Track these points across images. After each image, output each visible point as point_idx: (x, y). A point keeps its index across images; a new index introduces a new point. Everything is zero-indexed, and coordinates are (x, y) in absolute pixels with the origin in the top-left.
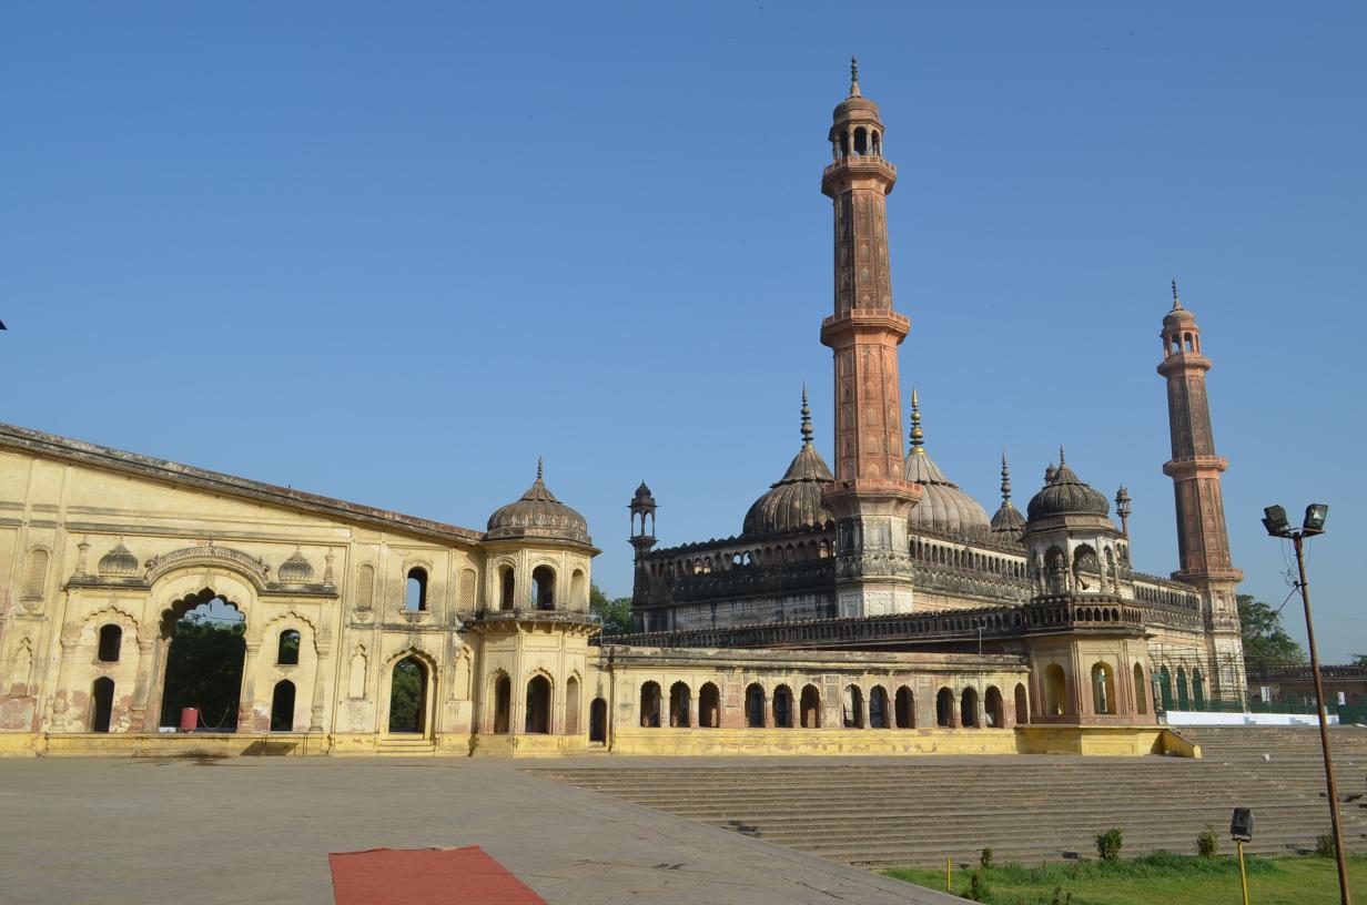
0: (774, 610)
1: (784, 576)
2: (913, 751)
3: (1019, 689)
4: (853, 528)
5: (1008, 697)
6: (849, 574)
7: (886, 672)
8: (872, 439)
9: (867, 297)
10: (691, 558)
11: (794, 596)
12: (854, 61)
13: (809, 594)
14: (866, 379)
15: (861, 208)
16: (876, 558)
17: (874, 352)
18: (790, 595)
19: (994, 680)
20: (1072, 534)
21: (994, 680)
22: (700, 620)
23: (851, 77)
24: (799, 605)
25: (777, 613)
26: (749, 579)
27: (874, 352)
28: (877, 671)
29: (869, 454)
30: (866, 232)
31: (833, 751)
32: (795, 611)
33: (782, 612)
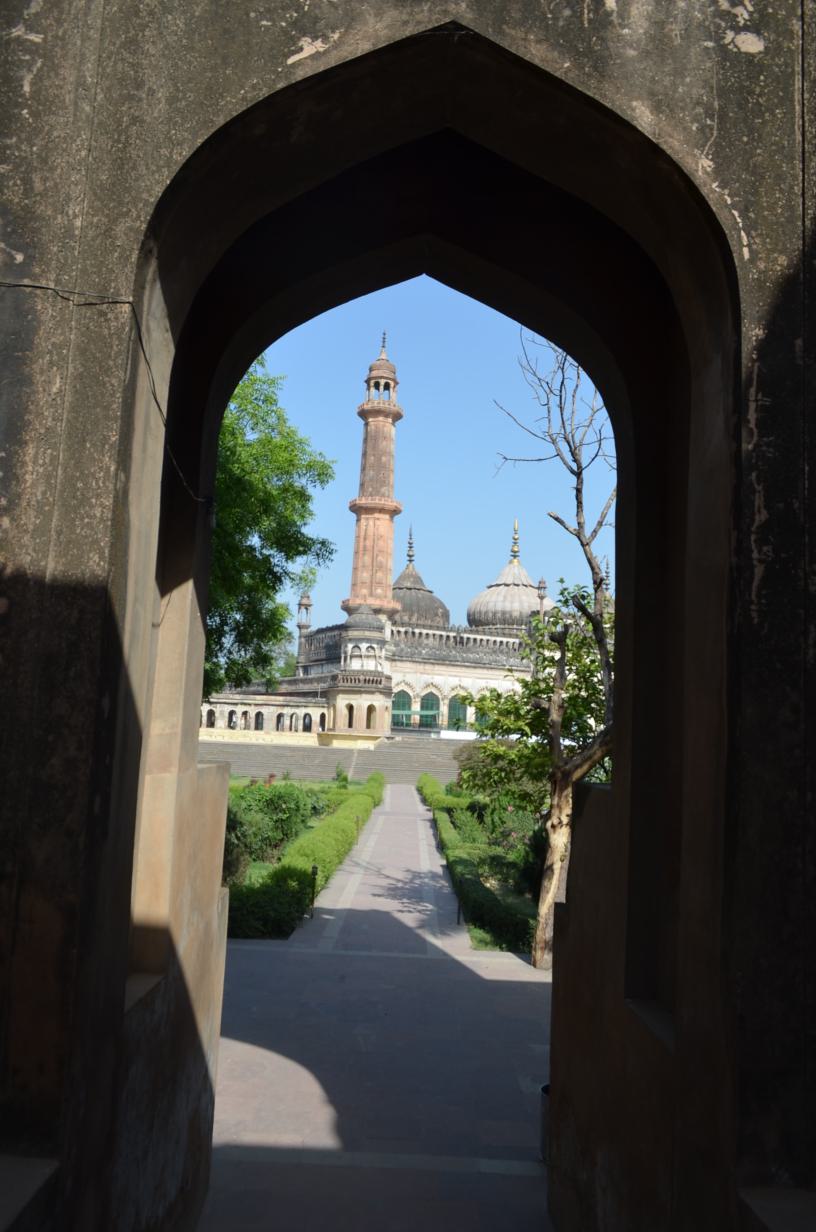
2: (261, 742)
3: (323, 716)
5: (316, 719)
7: (250, 705)
8: (365, 575)
9: (370, 489)
14: (365, 539)
15: (373, 434)
17: (371, 523)
19: (309, 710)
20: (350, 640)
21: (309, 710)
27: (371, 523)
28: (245, 704)
30: (374, 448)
31: (220, 739)
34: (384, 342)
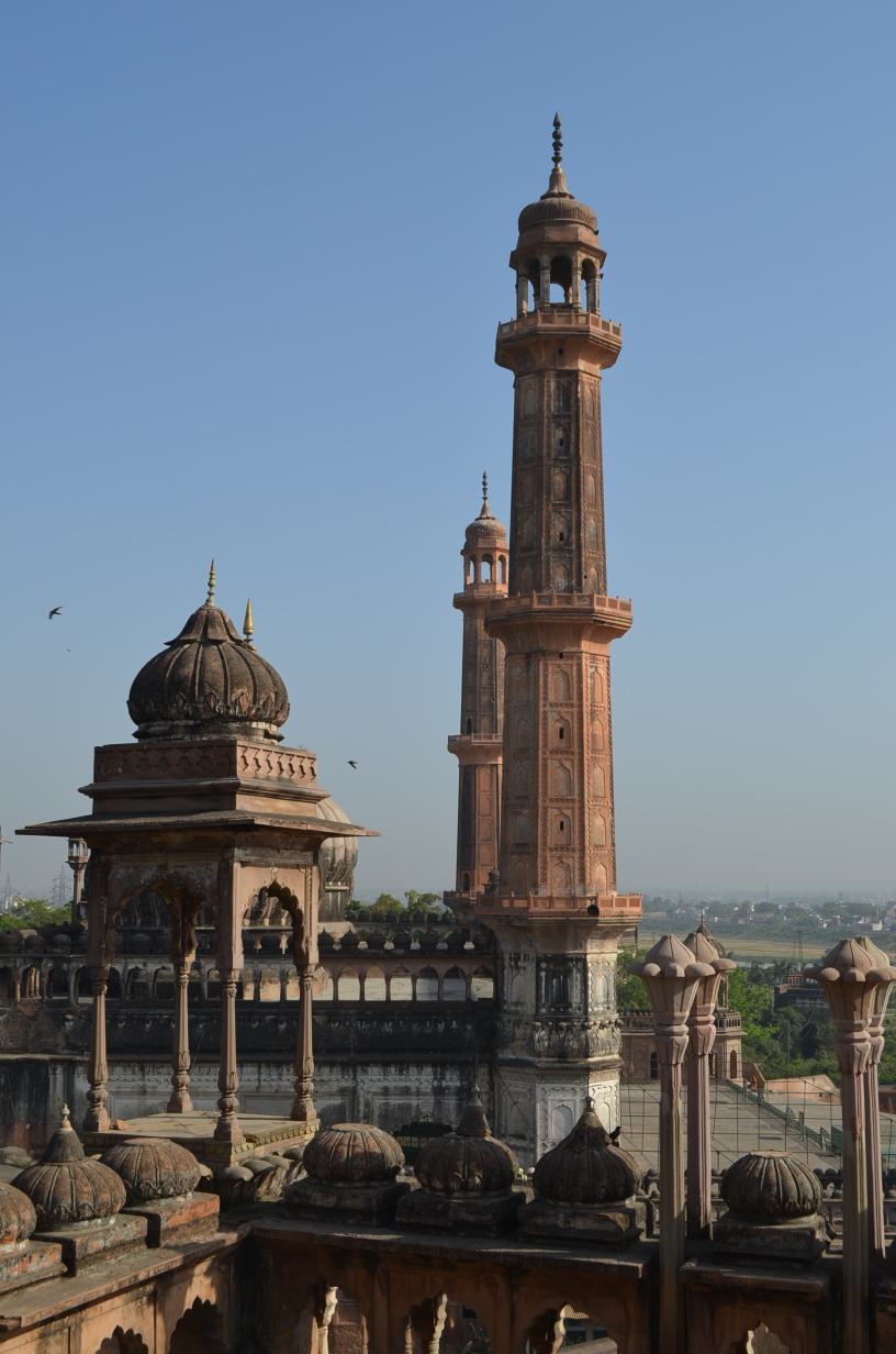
0: (335, 1087)
1: (365, 1026)
4: (568, 973)
6: (562, 1053)
10: (119, 968)
11: (385, 1065)
12: (557, 124)
13: (420, 1065)
16: (602, 1026)
18: (376, 1063)
22: (143, 1092)
23: (552, 153)
24: (394, 1080)
25: (342, 1092)
26: (276, 1022)
29: (597, 846)
32: (386, 1092)
33: (354, 1091)
34: (557, 146)
